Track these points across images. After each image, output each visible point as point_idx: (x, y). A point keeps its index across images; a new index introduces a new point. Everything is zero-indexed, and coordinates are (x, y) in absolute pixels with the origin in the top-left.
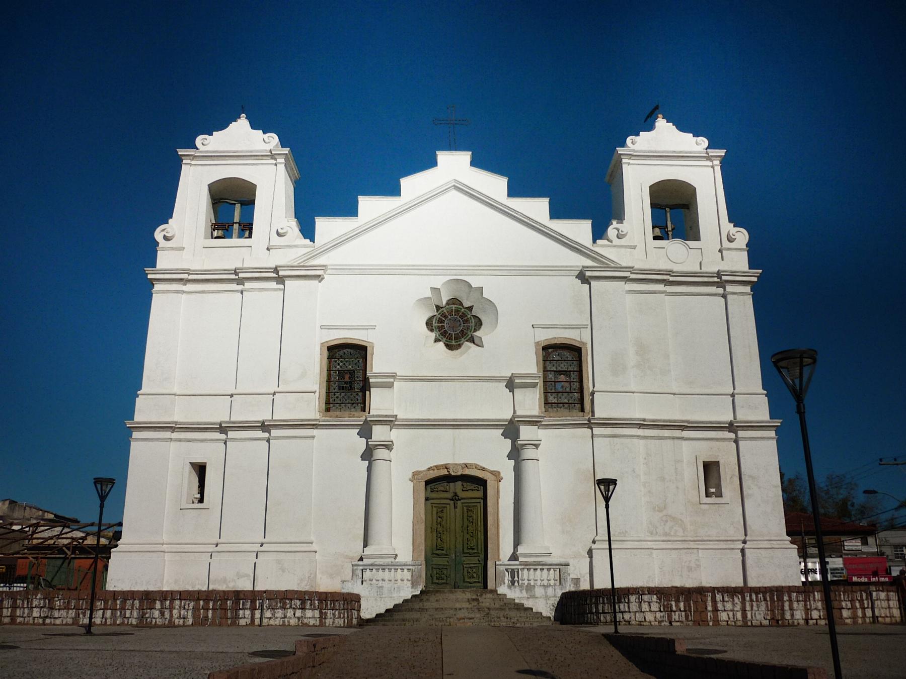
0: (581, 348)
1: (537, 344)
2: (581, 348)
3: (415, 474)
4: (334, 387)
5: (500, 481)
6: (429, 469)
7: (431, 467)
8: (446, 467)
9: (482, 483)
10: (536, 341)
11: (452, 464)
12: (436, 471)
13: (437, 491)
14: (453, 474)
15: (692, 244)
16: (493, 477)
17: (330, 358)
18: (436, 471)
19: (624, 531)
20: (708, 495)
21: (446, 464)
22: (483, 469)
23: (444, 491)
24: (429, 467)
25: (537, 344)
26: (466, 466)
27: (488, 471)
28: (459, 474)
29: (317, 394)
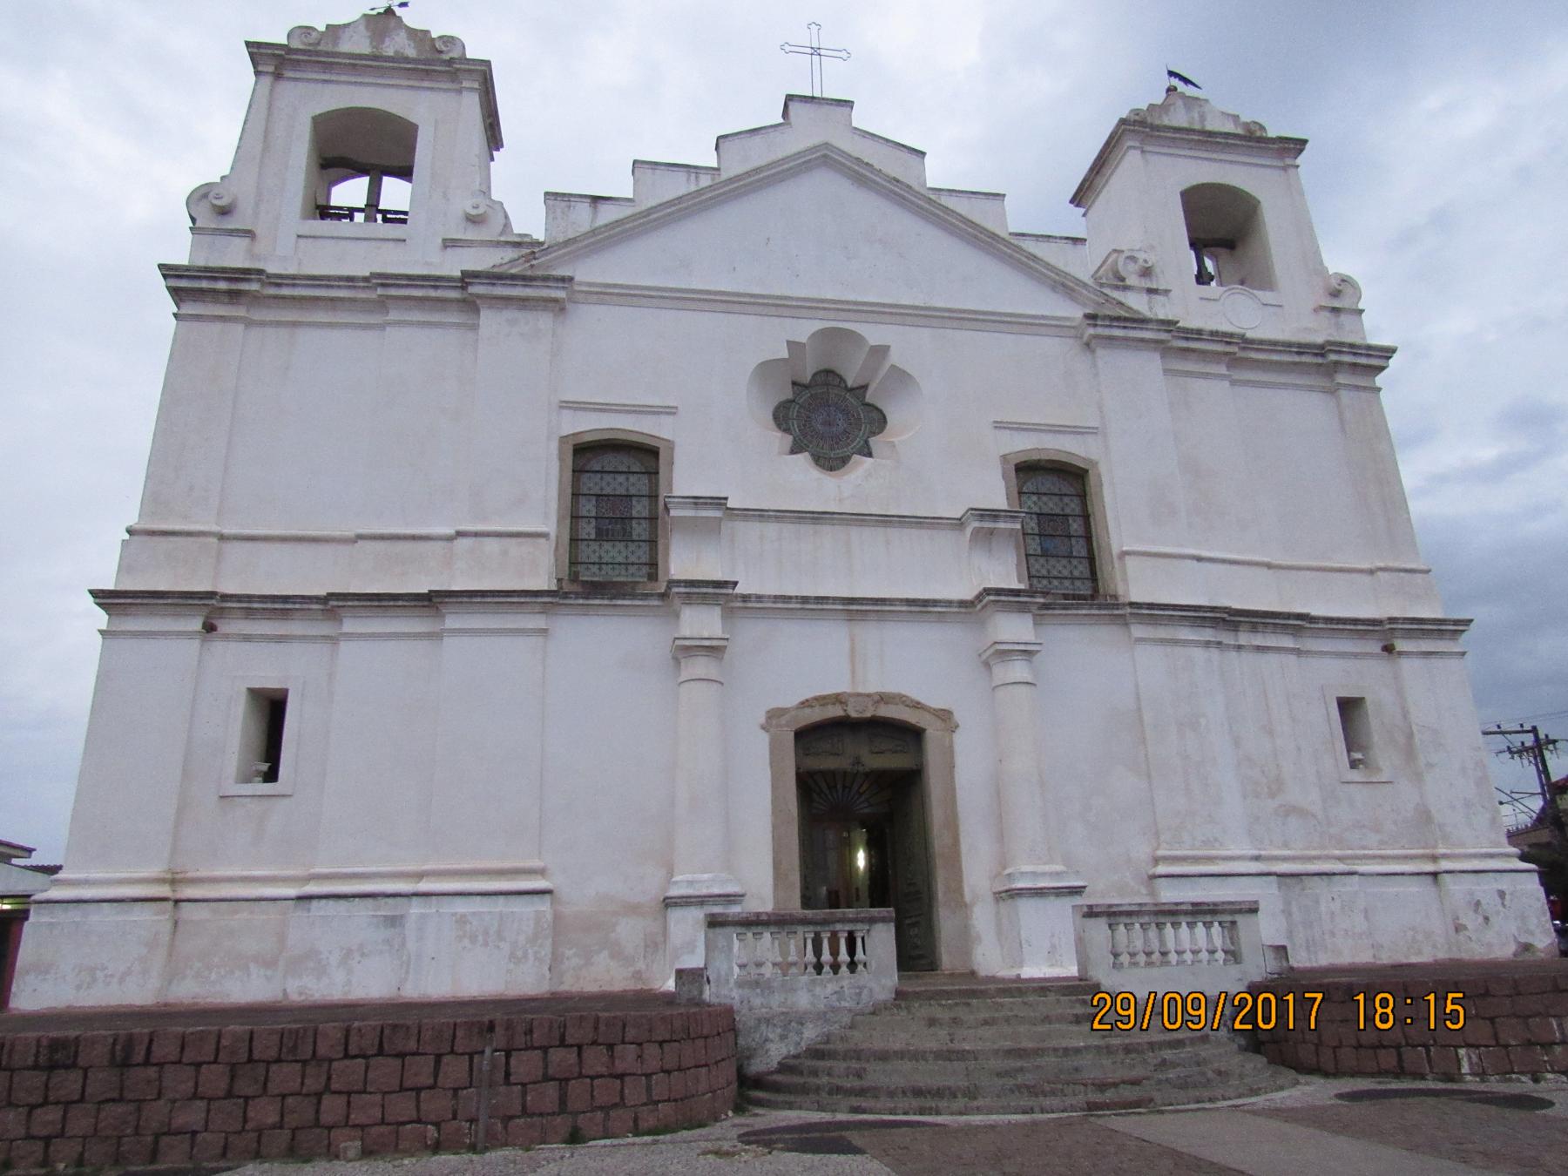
0: (1087, 471)
1: (1004, 458)
2: (1087, 471)
3: (774, 715)
4: (588, 530)
6: (803, 703)
7: (807, 701)
8: (838, 699)
9: (910, 735)
11: (851, 695)
12: (817, 709)
14: (854, 714)
15: (1267, 296)
16: (939, 723)
17: (577, 471)
18: (817, 709)
20: (1354, 764)
21: (838, 695)
22: (917, 706)
23: (832, 754)
25: (1004, 458)
26: (883, 698)
27: (929, 712)
28: (868, 714)
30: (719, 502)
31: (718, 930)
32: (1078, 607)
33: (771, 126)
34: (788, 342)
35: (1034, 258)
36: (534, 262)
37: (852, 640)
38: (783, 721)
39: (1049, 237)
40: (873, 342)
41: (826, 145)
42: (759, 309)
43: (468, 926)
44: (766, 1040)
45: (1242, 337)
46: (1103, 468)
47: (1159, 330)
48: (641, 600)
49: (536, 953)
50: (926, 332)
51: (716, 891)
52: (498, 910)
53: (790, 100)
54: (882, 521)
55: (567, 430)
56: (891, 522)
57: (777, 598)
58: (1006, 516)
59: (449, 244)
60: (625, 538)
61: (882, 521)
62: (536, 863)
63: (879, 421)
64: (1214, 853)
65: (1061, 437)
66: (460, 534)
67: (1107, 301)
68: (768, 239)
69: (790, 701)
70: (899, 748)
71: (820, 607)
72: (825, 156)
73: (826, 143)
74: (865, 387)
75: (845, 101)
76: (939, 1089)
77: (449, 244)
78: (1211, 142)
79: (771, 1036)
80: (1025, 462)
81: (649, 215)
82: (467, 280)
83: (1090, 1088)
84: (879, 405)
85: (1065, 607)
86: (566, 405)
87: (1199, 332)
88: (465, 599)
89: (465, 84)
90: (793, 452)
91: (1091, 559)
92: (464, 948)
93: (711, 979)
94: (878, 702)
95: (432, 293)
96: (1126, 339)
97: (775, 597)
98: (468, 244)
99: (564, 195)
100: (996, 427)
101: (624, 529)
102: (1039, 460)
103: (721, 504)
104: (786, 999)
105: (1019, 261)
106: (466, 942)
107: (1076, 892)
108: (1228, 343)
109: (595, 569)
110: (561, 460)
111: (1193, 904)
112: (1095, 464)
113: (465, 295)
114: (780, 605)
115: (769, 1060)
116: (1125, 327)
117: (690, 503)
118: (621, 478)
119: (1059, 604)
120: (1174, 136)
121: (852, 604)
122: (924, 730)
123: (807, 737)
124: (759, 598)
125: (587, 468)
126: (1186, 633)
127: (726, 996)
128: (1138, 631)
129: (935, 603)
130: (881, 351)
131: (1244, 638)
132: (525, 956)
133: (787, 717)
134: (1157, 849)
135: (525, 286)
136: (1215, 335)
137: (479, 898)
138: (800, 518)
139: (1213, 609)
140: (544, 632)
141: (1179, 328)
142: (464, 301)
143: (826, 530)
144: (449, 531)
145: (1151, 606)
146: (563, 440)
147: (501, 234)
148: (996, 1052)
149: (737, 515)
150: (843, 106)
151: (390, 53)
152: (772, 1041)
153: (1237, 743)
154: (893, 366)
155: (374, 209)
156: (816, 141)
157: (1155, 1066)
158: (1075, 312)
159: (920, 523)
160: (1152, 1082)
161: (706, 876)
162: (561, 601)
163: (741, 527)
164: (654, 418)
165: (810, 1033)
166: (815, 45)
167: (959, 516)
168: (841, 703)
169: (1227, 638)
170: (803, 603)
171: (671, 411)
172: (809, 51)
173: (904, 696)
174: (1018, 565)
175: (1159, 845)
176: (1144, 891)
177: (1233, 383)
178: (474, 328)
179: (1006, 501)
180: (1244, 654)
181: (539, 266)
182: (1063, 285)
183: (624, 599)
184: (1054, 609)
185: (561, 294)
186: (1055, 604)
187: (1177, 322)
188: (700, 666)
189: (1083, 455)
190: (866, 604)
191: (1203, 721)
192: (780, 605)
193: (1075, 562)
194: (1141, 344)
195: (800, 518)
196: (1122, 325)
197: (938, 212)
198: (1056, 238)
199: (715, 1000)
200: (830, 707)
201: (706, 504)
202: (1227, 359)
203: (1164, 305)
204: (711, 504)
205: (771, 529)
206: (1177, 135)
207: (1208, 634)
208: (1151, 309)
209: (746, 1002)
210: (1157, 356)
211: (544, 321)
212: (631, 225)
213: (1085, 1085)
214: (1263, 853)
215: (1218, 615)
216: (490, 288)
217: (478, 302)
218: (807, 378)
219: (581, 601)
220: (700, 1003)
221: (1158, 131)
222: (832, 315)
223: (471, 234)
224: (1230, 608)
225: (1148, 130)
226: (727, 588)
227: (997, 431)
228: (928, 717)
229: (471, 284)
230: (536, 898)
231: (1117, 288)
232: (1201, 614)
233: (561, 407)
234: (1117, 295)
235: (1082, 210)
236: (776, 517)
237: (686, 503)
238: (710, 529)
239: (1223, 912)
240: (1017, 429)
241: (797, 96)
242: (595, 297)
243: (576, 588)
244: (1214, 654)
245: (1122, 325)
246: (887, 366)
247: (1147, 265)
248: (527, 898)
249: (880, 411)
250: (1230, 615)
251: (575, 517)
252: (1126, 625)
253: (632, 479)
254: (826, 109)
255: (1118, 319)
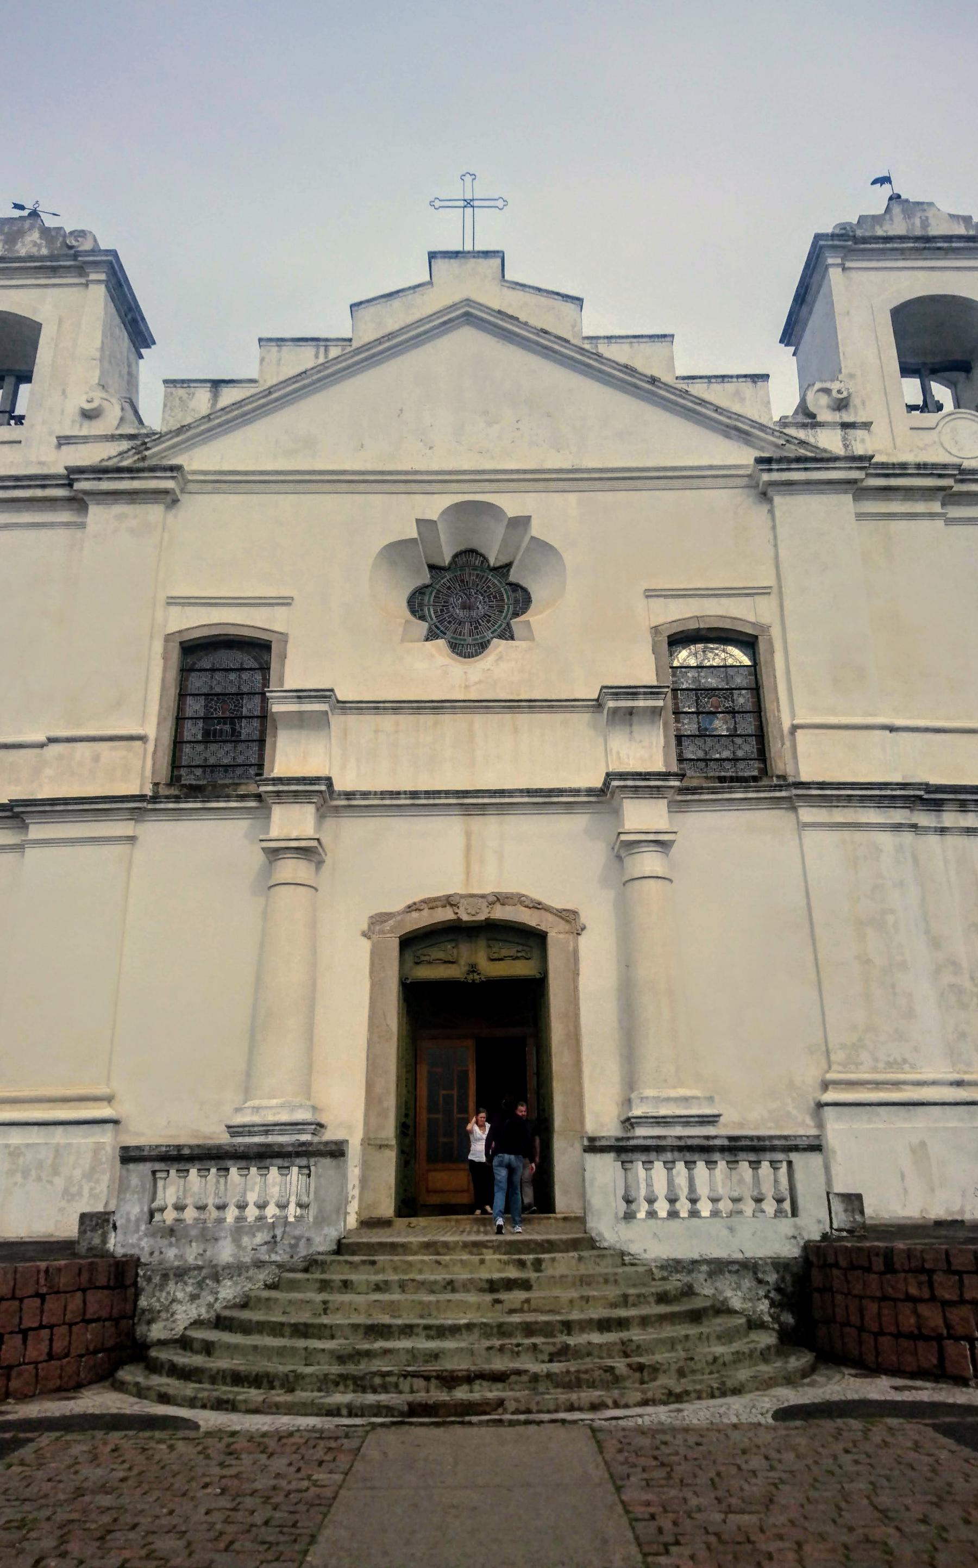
1: (656, 630)
2: (756, 637)
3: (378, 920)
4: (192, 731)
5: (578, 934)
6: (409, 907)
7: (415, 904)
8: (449, 902)
10: (652, 625)
11: (462, 896)
12: (425, 913)
13: (430, 963)
14: (465, 918)
16: (563, 926)
17: (185, 671)
18: (425, 913)
19: (899, 1060)
21: (450, 896)
22: (538, 906)
24: (410, 902)
25: (656, 630)
26: (500, 899)
28: (481, 917)
29: (151, 746)
30: (323, 695)
31: (132, 1166)
32: (731, 790)
33: (410, 288)
34: (418, 521)
35: (703, 402)
36: (147, 453)
37: (468, 835)
38: (387, 926)
39: (723, 377)
40: (511, 513)
41: (468, 301)
42: (386, 487)
43: (21, 1160)
44: (173, 1301)
45: (958, 467)
46: (775, 632)
47: (851, 468)
48: (237, 801)
49: (91, 1189)
50: (572, 497)
51: (284, 1117)
52: (55, 1141)
53: (433, 257)
54: (509, 707)
55: (173, 627)
56: (519, 707)
57: (383, 794)
58: (645, 693)
59: (64, 441)
60: (233, 738)
61: (509, 707)
62: (102, 1090)
63: (522, 598)
64: (902, 1077)
65: (724, 601)
66: (52, 740)
67: (788, 441)
68: (401, 410)
69: (397, 905)
70: (519, 954)
71: (431, 801)
72: (467, 314)
73: (467, 300)
74: (509, 565)
75: (494, 252)
76: (257, 1375)
77: (64, 441)
78: (929, 249)
79: (180, 1295)
80: (682, 632)
81: (270, 393)
82: (71, 477)
83: (434, 1382)
84: (523, 583)
85: (714, 791)
86: (172, 601)
87: (903, 466)
88: (48, 808)
89: (93, 277)
90: (427, 640)
91: (761, 737)
92: (16, 1184)
93: (118, 1224)
94: (493, 903)
95: (39, 493)
96: (808, 483)
97: (382, 793)
98: (85, 439)
99: (183, 381)
100: (647, 597)
101: (233, 730)
102: (699, 630)
103: (325, 697)
104: (205, 1251)
105: (684, 407)
106: (18, 1177)
107: (709, 1122)
108: (940, 476)
109: (199, 772)
110: (165, 658)
111: (731, 1138)
112: (765, 628)
113: (72, 494)
114: (388, 802)
115: (173, 1325)
116: (806, 469)
117: (292, 697)
118: (232, 676)
119: (708, 788)
120: (881, 246)
121: (466, 797)
122: (547, 933)
123: (409, 942)
124: (365, 794)
125: (197, 667)
126: (871, 815)
127: (133, 1246)
128: (807, 814)
129: (560, 792)
130: (522, 523)
131: (950, 818)
132: (80, 1193)
133: (391, 922)
134: (827, 1072)
135: (132, 478)
136: (923, 469)
137: (36, 1128)
138: (418, 708)
139: (904, 786)
140: (132, 839)
141: (877, 464)
142: (70, 500)
143: (447, 719)
144: (41, 737)
145: (822, 785)
146: (168, 638)
147: (117, 428)
148: (355, 1327)
149: (351, 708)
150: (492, 257)
151: (23, 252)
152: (180, 1302)
153: (935, 943)
154: (532, 538)
155: (7, 415)
156: (457, 298)
157: (551, 1354)
158: (744, 456)
159: (552, 707)
160: (525, 1378)
161: (274, 1102)
162: (150, 806)
163: (352, 720)
164: (269, 609)
165: (228, 1291)
166: (469, 196)
167: (596, 697)
168: (452, 905)
169: (924, 819)
170: (413, 798)
171: (285, 602)
172: (462, 203)
173: (524, 896)
174: (666, 746)
175: (830, 1067)
176: (809, 1121)
177: (950, 522)
178: (83, 526)
179: (655, 677)
180: (950, 840)
181: (154, 455)
182: (737, 429)
183: (218, 801)
184: (701, 793)
185: (170, 484)
186: (702, 788)
187: (872, 457)
188: (290, 869)
189: (752, 619)
190: (483, 797)
191: (890, 919)
192: (388, 802)
193: (739, 741)
194: (826, 487)
195: (418, 708)
196: (802, 466)
197: (591, 362)
198: (731, 377)
199: (120, 1251)
200: (440, 909)
201: (310, 697)
202: (943, 493)
203: (863, 441)
204: (316, 697)
205: (387, 721)
206: (888, 245)
207: (899, 816)
208: (846, 446)
209: (157, 1253)
210: (848, 498)
211: (154, 512)
212: (250, 407)
213: (427, 1379)
214: (967, 1077)
215: (912, 793)
216: (96, 483)
217: (86, 498)
218: (446, 558)
219: (171, 806)
220: (106, 1254)
221: (864, 243)
222: (465, 487)
223: (88, 429)
224: (927, 784)
225: (850, 243)
226: (319, 784)
227: (650, 600)
228: (551, 918)
229: (77, 480)
230: (96, 1128)
231: (804, 426)
232: (889, 792)
233: (169, 604)
234: (801, 434)
235: (792, 349)
236: (393, 709)
237: (285, 697)
238: (320, 722)
239: (773, 1149)
240: (673, 596)
241: (441, 252)
242: (210, 486)
243: (174, 791)
244: (908, 838)
245: (802, 466)
246: (527, 539)
247: (841, 396)
248: (85, 1126)
249: (525, 590)
250: (928, 792)
251: (179, 720)
252: (794, 809)
253: (245, 676)
254: (472, 262)
255: (798, 460)
